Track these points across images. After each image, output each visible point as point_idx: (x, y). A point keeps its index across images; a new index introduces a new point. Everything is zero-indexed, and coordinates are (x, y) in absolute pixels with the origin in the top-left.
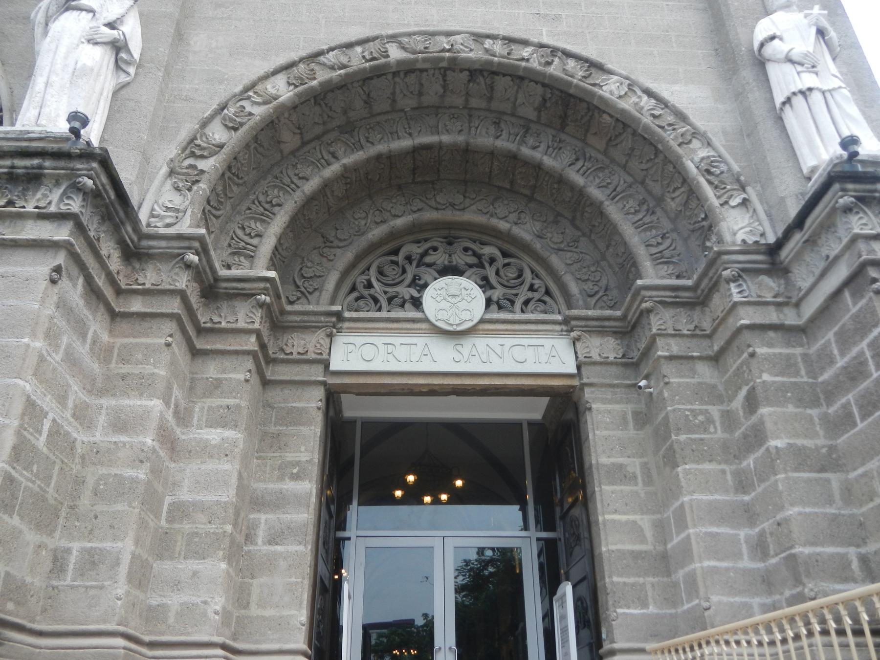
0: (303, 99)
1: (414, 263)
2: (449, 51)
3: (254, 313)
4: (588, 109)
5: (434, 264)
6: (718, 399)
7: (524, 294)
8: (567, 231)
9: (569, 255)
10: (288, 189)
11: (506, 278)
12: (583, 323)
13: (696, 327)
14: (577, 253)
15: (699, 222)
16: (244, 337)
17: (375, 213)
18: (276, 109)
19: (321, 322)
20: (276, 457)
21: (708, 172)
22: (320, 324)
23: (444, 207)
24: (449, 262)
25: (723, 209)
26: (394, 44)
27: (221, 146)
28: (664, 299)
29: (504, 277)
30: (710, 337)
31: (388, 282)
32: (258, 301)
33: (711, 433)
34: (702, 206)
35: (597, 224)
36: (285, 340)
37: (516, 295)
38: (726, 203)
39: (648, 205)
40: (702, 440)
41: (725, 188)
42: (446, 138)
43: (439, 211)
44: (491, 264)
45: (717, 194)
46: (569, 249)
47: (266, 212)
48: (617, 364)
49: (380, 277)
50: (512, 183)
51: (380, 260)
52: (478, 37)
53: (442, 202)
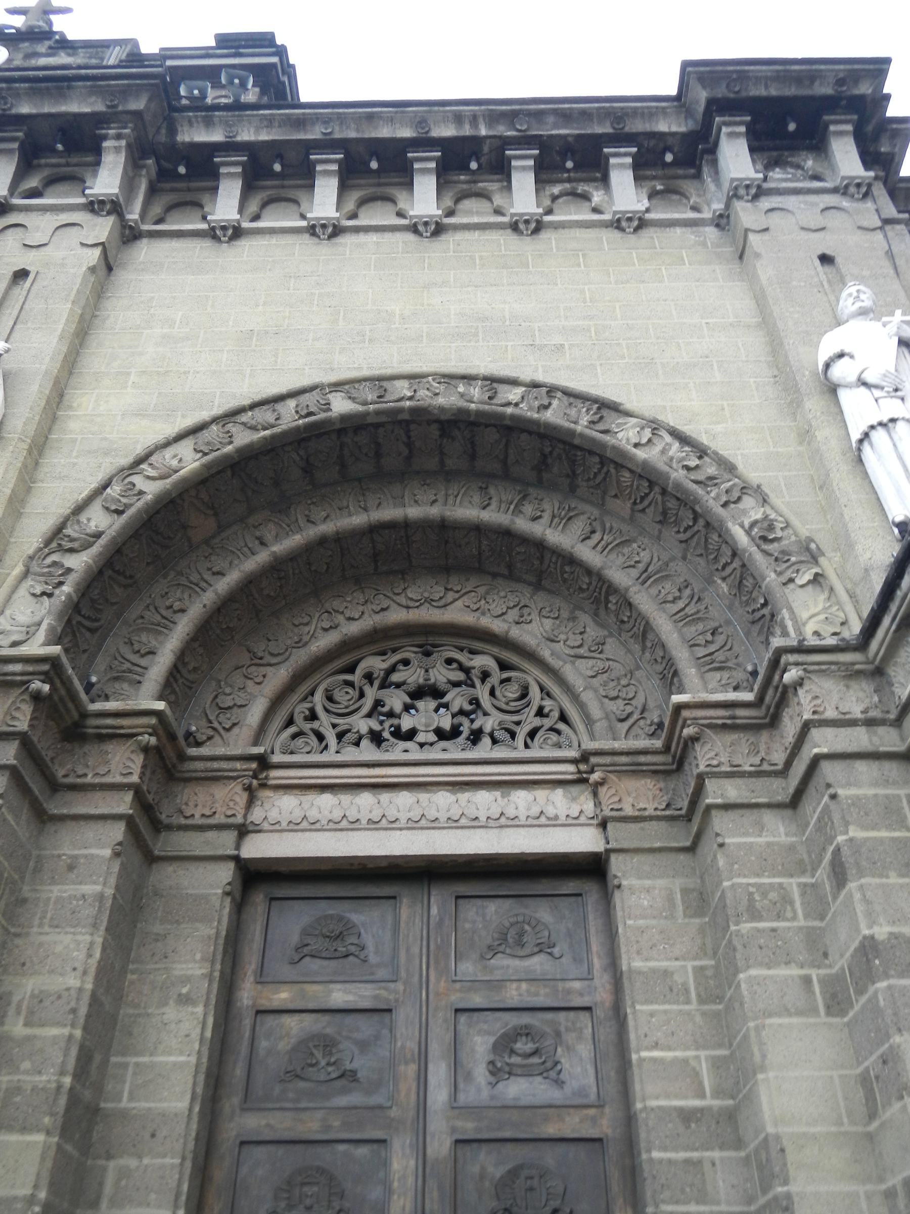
0: (214, 471)
1: (376, 683)
2: (411, 398)
3: (132, 760)
4: (602, 464)
5: (404, 683)
6: (801, 868)
7: (530, 720)
8: (588, 629)
9: (591, 662)
10: (197, 589)
11: (504, 700)
12: (608, 760)
13: (763, 760)
15: (759, 609)
16: (116, 795)
18: (175, 485)
19: (236, 770)
20: (159, 969)
21: (764, 539)
23: (418, 604)
24: (426, 680)
25: (787, 591)
26: (339, 394)
27: (98, 535)
28: (714, 721)
30: (784, 772)
31: (331, 709)
32: (139, 742)
33: (788, 920)
34: (760, 587)
35: (626, 619)
36: (185, 798)
37: (518, 723)
38: (791, 580)
39: (693, 590)
40: (774, 930)
41: (788, 560)
42: (414, 512)
43: (410, 610)
45: (778, 569)
46: (592, 654)
47: (164, 621)
48: (658, 818)
50: (510, 567)
52: (450, 378)
53: (415, 598)
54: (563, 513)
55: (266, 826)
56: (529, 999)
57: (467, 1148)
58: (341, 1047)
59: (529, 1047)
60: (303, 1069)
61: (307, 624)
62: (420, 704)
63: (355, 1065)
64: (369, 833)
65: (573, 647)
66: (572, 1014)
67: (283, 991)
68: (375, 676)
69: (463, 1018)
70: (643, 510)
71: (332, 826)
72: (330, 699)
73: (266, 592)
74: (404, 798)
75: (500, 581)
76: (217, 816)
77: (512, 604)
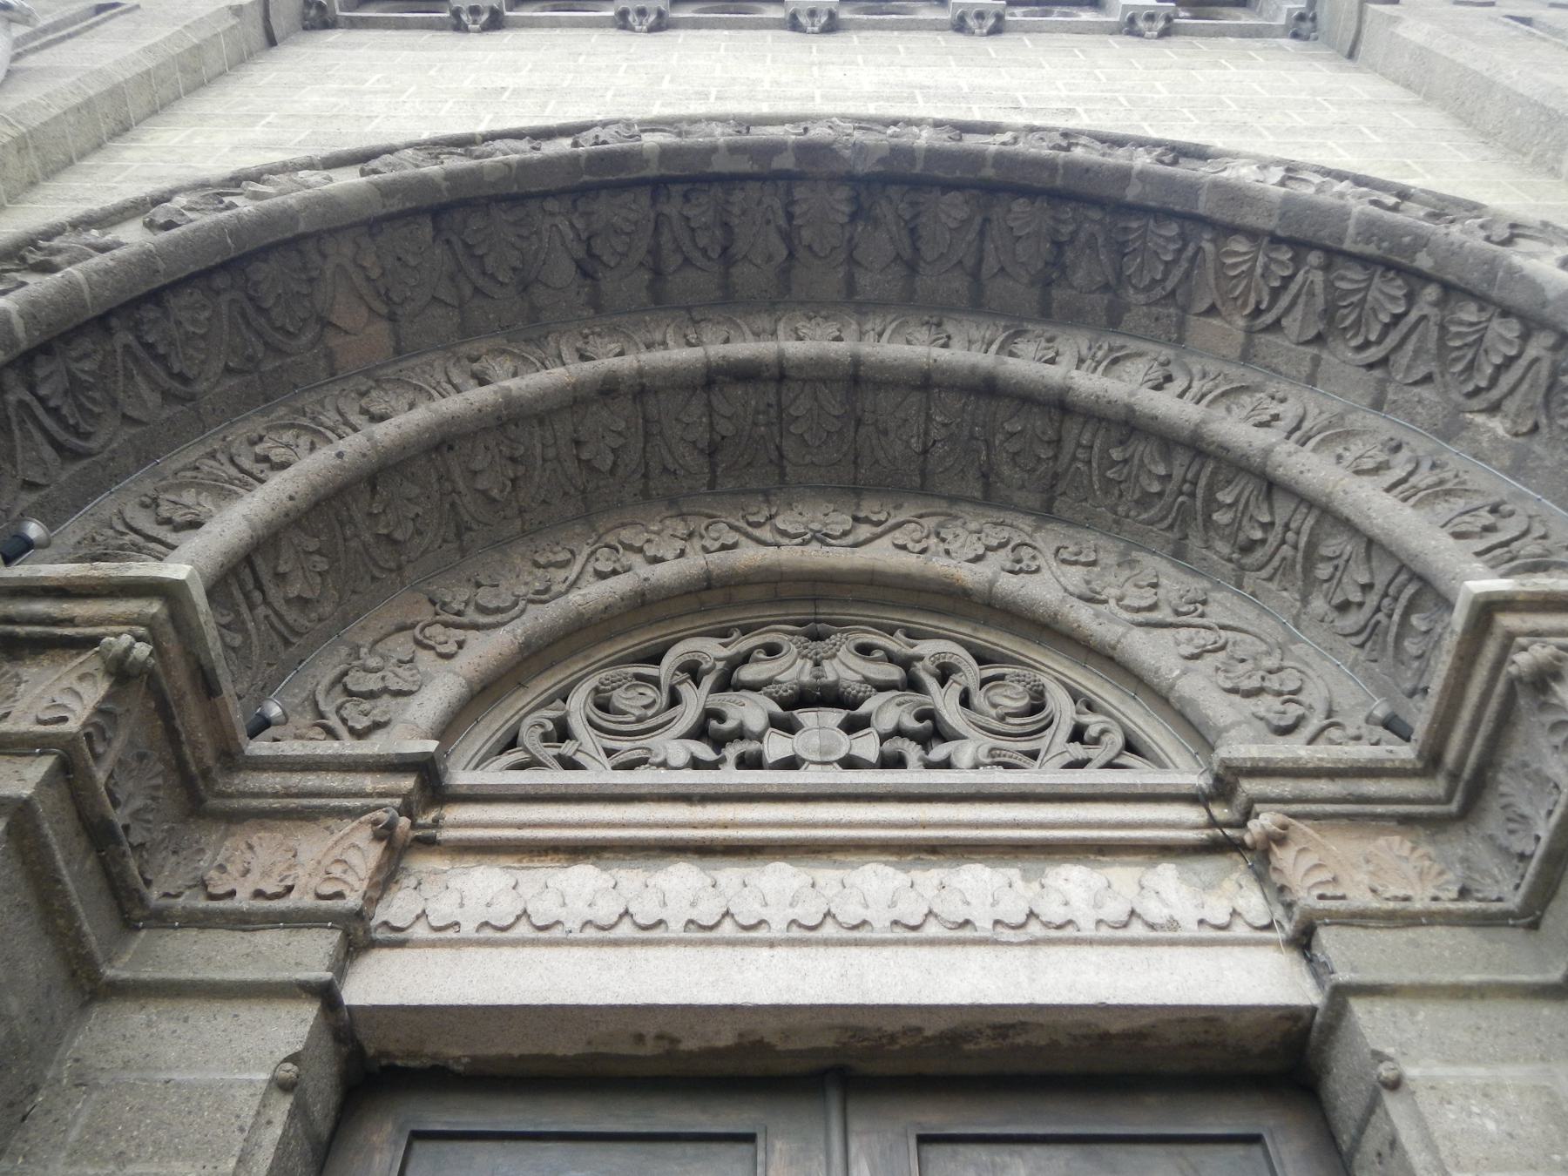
0: (395, 205)
1: (708, 682)
3: (77, 694)
5: (769, 682)
8: (1164, 581)
9: (1184, 633)
12: (1286, 787)
14: (1209, 628)
17: (598, 555)
22: (358, 803)
29: (985, 706)
42: (794, 349)
44: (943, 680)
49: (599, 717)
51: (604, 675)
53: (791, 530)
54: (1100, 354)
61: (564, 564)
62: (806, 717)
64: (690, 951)
65: (1138, 610)
68: (705, 666)
70: (1276, 326)
71: (591, 933)
72: (604, 706)
73: (482, 483)
74: (778, 877)
75: (965, 510)
76: (294, 895)
77: (995, 543)
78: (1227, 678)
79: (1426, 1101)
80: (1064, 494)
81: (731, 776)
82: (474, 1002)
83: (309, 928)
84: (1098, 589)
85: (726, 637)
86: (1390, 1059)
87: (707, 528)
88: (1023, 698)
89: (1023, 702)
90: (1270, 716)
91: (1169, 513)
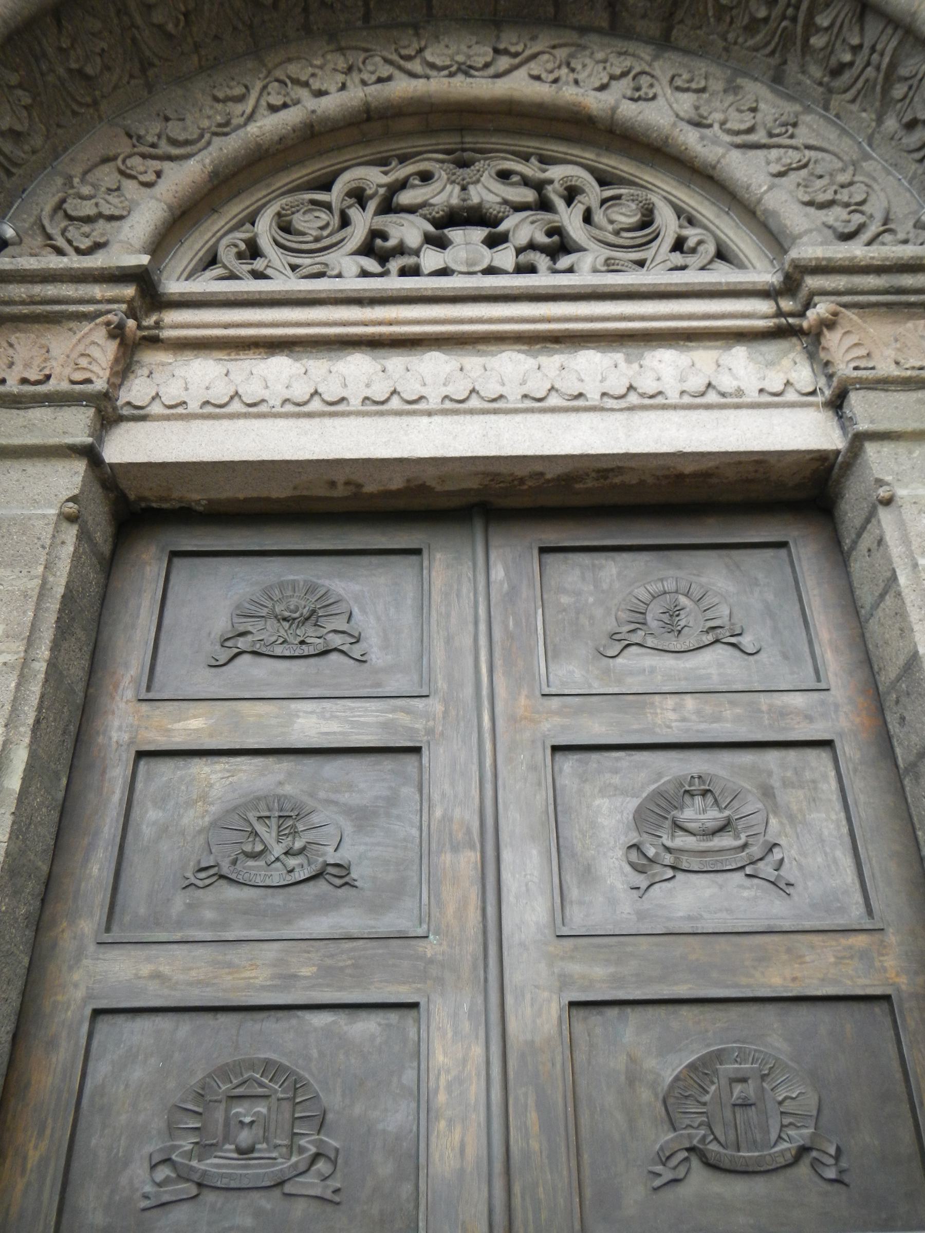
1: (372, 206)
5: (424, 204)
8: (762, 106)
9: (774, 153)
11: (610, 228)
12: (840, 282)
14: (796, 148)
17: (269, 89)
22: (91, 308)
46: (775, 140)
49: (282, 237)
51: (284, 201)
53: (439, 62)
55: (156, 409)
56: (703, 726)
57: (595, 1018)
58: (316, 819)
59: (712, 816)
60: (234, 862)
61: (241, 99)
62: (455, 234)
63: (345, 855)
64: (367, 421)
65: (738, 133)
66: (792, 755)
67: (195, 717)
68: (369, 192)
69: (569, 764)
71: (289, 408)
72: (286, 228)
73: (158, 17)
75: (593, 40)
76: (52, 381)
77: (618, 72)
78: (806, 192)
79: (908, 512)
80: (681, 21)
81: (395, 283)
82: (205, 459)
83: (69, 406)
84: (705, 114)
85: (386, 165)
86: (888, 484)
87: (364, 62)
88: (635, 215)
89: (635, 219)
90: (837, 225)
91: (773, 37)
